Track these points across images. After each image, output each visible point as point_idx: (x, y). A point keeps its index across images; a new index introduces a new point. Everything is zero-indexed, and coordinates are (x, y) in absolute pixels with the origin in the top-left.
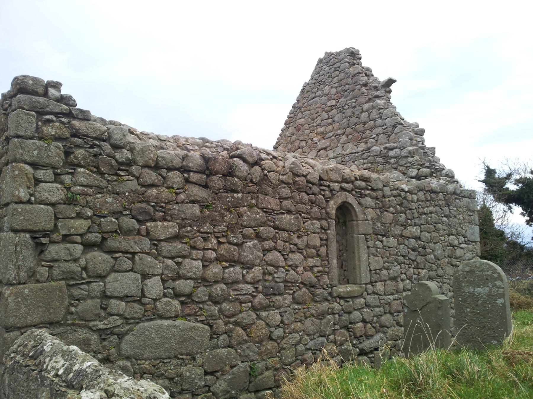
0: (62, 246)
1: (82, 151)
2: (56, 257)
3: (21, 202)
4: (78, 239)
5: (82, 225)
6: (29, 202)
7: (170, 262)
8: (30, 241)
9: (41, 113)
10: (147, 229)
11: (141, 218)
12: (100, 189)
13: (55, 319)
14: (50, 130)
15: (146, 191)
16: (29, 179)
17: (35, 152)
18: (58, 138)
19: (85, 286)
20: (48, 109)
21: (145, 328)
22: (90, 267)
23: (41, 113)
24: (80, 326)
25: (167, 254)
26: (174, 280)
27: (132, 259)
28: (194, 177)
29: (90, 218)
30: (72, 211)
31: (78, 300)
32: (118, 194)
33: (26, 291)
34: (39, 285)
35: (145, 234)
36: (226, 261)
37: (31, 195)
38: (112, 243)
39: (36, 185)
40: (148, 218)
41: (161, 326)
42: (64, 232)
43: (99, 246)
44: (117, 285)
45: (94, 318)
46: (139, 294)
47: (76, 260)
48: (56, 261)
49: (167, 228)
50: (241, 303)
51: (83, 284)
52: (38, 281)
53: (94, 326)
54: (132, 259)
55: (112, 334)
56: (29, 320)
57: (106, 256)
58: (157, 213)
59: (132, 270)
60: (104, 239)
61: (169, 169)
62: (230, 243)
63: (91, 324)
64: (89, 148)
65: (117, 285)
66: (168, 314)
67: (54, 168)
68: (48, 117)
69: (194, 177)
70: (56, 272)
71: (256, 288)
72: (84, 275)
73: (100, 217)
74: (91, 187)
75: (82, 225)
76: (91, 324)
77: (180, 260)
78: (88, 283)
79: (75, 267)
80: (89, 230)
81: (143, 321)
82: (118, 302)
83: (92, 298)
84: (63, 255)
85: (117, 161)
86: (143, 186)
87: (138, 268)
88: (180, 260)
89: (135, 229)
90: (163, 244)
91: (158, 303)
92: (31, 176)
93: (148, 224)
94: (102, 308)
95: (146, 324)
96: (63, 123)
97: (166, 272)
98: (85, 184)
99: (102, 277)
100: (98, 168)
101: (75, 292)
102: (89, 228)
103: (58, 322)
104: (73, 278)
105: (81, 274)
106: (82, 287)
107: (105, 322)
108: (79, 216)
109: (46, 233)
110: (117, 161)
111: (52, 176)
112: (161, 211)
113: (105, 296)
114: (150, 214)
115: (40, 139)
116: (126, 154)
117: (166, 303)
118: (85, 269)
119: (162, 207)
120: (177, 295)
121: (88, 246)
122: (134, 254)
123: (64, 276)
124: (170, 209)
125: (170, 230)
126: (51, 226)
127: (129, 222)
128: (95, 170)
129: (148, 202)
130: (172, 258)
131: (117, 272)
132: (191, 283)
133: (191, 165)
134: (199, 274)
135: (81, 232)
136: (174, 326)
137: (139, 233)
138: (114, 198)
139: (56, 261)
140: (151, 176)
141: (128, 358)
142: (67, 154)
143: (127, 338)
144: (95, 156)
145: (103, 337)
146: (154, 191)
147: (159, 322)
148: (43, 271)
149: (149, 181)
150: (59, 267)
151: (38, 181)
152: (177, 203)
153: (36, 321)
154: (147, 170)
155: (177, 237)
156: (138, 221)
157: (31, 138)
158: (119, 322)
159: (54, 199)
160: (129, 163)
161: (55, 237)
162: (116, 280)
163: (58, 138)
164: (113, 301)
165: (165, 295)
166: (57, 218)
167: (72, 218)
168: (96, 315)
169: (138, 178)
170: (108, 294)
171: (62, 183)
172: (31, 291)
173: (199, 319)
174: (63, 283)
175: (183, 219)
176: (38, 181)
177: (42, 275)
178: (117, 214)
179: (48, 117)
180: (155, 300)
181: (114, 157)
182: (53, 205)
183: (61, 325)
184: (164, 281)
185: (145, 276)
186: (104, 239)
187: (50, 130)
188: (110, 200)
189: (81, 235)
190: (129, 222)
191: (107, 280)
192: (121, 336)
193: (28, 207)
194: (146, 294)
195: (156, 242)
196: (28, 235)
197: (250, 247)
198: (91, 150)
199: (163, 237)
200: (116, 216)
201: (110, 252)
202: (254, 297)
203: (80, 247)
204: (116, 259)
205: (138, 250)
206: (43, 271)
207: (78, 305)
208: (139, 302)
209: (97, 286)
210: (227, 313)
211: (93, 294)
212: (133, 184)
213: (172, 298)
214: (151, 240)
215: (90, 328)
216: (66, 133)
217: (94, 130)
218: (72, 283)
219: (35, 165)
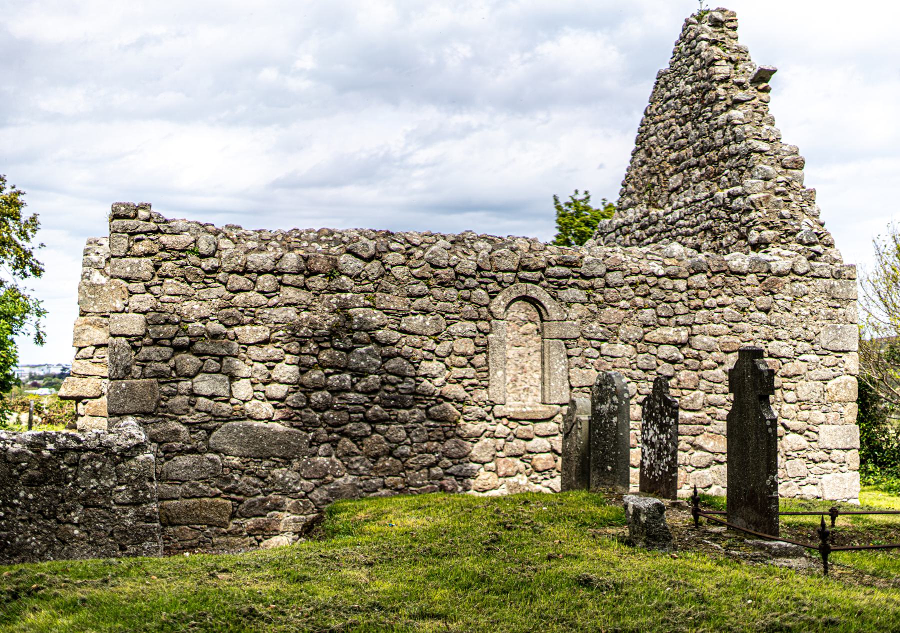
0: (152, 348)
3: (117, 312)
6: (123, 311)
10: (235, 334)
11: (228, 322)
12: (188, 297)
19: (175, 384)
22: (179, 368)
28: (288, 279)
29: (178, 323)
32: (204, 300)
36: (330, 367)
47: (166, 361)
50: (350, 413)
52: (133, 378)
57: (194, 359)
59: (219, 372)
61: (260, 273)
62: (336, 348)
63: (180, 417)
66: (258, 416)
69: (288, 279)
71: (372, 399)
76: (180, 417)
83: (181, 395)
86: (231, 292)
88: (272, 364)
99: (190, 377)
113: (192, 393)
118: (174, 368)
129: (236, 307)
132: (285, 388)
133: (284, 266)
134: (294, 379)
136: (265, 428)
140: (241, 281)
149: (237, 287)
150: (150, 366)
165: (254, 397)
169: (225, 284)
170: (196, 392)
173: (295, 424)
176: (131, 293)
180: (244, 401)
181: (200, 266)
186: (192, 343)
189: (171, 339)
194: (234, 394)
197: (361, 354)
201: (198, 354)
202: (368, 408)
203: (171, 350)
204: (204, 361)
210: (330, 422)
218: (162, 380)
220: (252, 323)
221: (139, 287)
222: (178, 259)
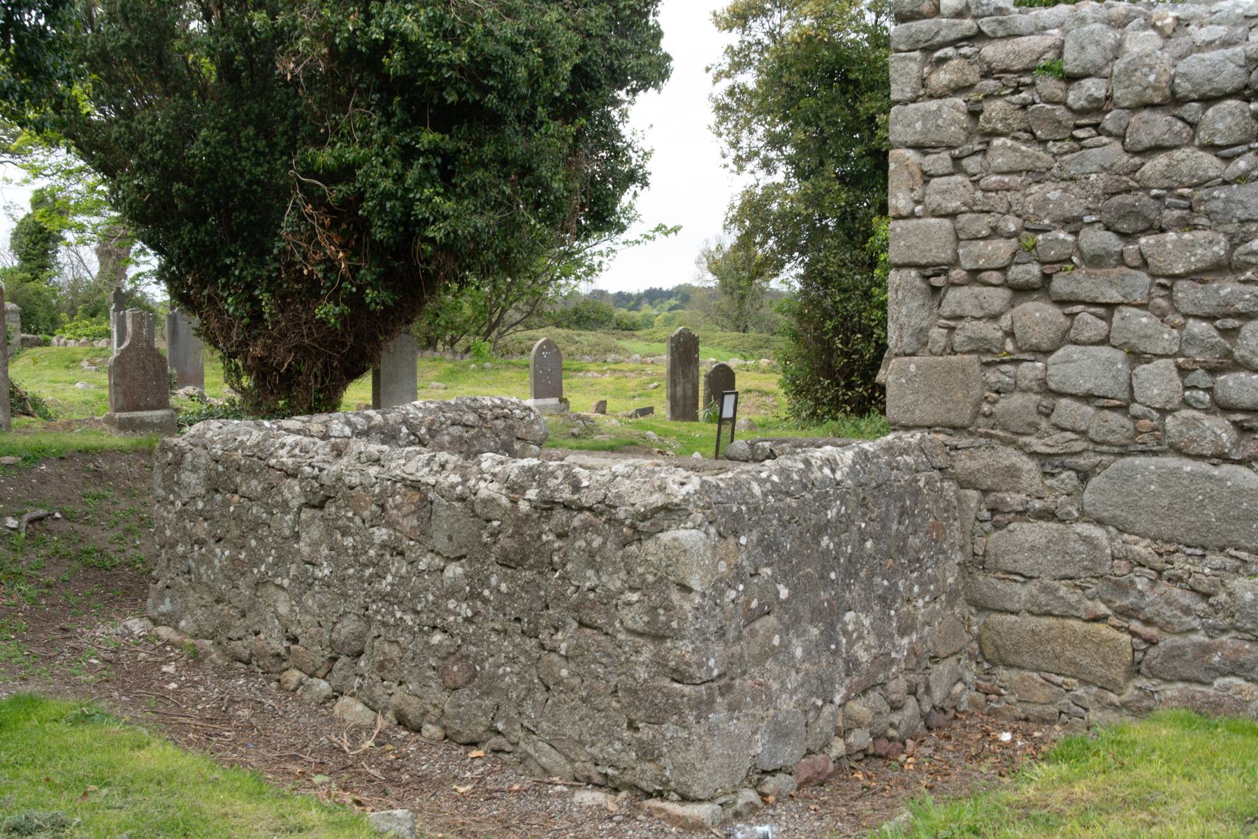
0: (965, 290)
1: (999, 103)
2: (959, 312)
4: (995, 277)
5: (1001, 249)
6: (912, 215)
7: (1198, 328)
8: (919, 283)
9: (929, 50)
11: (1124, 227)
12: (1038, 175)
13: (958, 422)
14: (942, 78)
15: (1143, 164)
16: (911, 175)
17: (919, 125)
18: (958, 90)
20: (939, 39)
21: (1133, 468)
22: (1018, 334)
23: (929, 50)
24: (1005, 442)
25: (1190, 309)
26: (1213, 371)
27: (1108, 319)
30: (982, 224)
31: (998, 392)
33: (912, 368)
34: (932, 358)
35: (1137, 263)
37: (918, 202)
38: (1060, 285)
39: (926, 182)
40: (1141, 225)
41: (1174, 472)
42: (969, 266)
43: (1040, 288)
44: (1070, 369)
45: (1026, 429)
46: (1126, 396)
47: (995, 317)
48: (960, 318)
49: (1193, 244)
51: (1003, 362)
52: (931, 353)
53: (1026, 445)
54: (1108, 319)
55: (1065, 467)
56: (917, 416)
57: (1052, 311)
58: (1166, 212)
59: (1105, 341)
60: (1047, 278)
64: (1013, 94)
65: (1070, 369)
67: (950, 147)
68: (939, 53)
70: (958, 338)
72: (1009, 346)
73: (1038, 231)
74: (1019, 172)
75: (1001, 249)
77: (1231, 323)
78: (1017, 362)
79: (992, 331)
80: (1013, 260)
81: (1129, 454)
82: (1076, 405)
83: (1024, 391)
84: (969, 308)
85: (1069, 108)
87: (1117, 338)
88: (1231, 323)
89: (1109, 254)
90: (1183, 284)
91: (1169, 419)
92: (914, 169)
93: (1143, 240)
94: (1040, 413)
95: (1139, 461)
96: (965, 57)
97: (1192, 351)
98: (1005, 169)
100: (1032, 133)
101: (992, 376)
102: (1014, 254)
103: (964, 428)
104: (989, 351)
105: (1003, 344)
106: (1004, 368)
107: (1047, 440)
108: (995, 232)
109: (941, 269)
110: (1069, 108)
111: (949, 162)
112: (1178, 207)
114: (1145, 218)
115: (931, 97)
116: (1093, 88)
117: (1185, 422)
118: (1010, 334)
119: (1182, 197)
120: (1226, 408)
121: (1021, 291)
122: (1111, 307)
123: (973, 346)
124: (1201, 201)
125: (1199, 251)
126: (945, 256)
127: (1096, 239)
128: (1026, 136)
129: (1146, 189)
130: (1210, 318)
131: (1076, 343)
135: (999, 263)
137: (1121, 260)
138: (1065, 190)
139: (960, 318)
141: (1100, 522)
142: (974, 114)
143: (1094, 481)
144: (1024, 107)
145: (1048, 469)
146: (1161, 160)
147: (1172, 461)
148: (937, 334)
149: (1146, 141)
151: (927, 177)
152: (1225, 183)
153: (929, 420)
154: (1145, 114)
155: (1221, 268)
156: (1123, 235)
157: (914, 101)
158: (1079, 446)
159: (953, 205)
160: (1098, 107)
161: (956, 274)
162: (1068, 360)
163: (958, 90)
164: (1064, 402)
165: (1186, 403)
166: (958, 240)
167: (984, 238)
168: (1030, 425)
169: (1121, 137)
170: (1053, 386)
171: (964, 172)
172: (918, 367)
174: (974, 357)
175: (1243, 222)
176: (927, 177)
177: (935, 342)
178: (1073, 224)
179: (939, 53)
180: (1163, 412)
181: (1063, 103)
182: (953, 215)
183: (971, 434)
184: (1182, 371)
185: (1137, 357)
186: (1047, 278)
187: (942, 78)
188: (1054, 195)
189: (1003, 269)
190: (1096, 239)
191: (1051, 359)
192: (1084, 476)
193: (913, 222)
194: (1136, 395)
195: (1167, 282)
196: (913, 273)
198: (1015, 98)
199: (1179, 269)
200: (1072, 227)
201: (1061, 303)
203: (1005, 294)
205: (1119, 299)
206: (937, 334)
207: (995, 402)
208: (1123, 409)
209: (1031, 370)
211: (1024, 384)
212: (1112, 152)
213: (1207, 411)
214: (1154, 276)
215: (1021, 448)
216: (972, 75)
217: (1018, 55)
218: (989, 358)
219: (920, 148)
220: (1185, 225)
221: (940, 161)
222: (1017, 91)
